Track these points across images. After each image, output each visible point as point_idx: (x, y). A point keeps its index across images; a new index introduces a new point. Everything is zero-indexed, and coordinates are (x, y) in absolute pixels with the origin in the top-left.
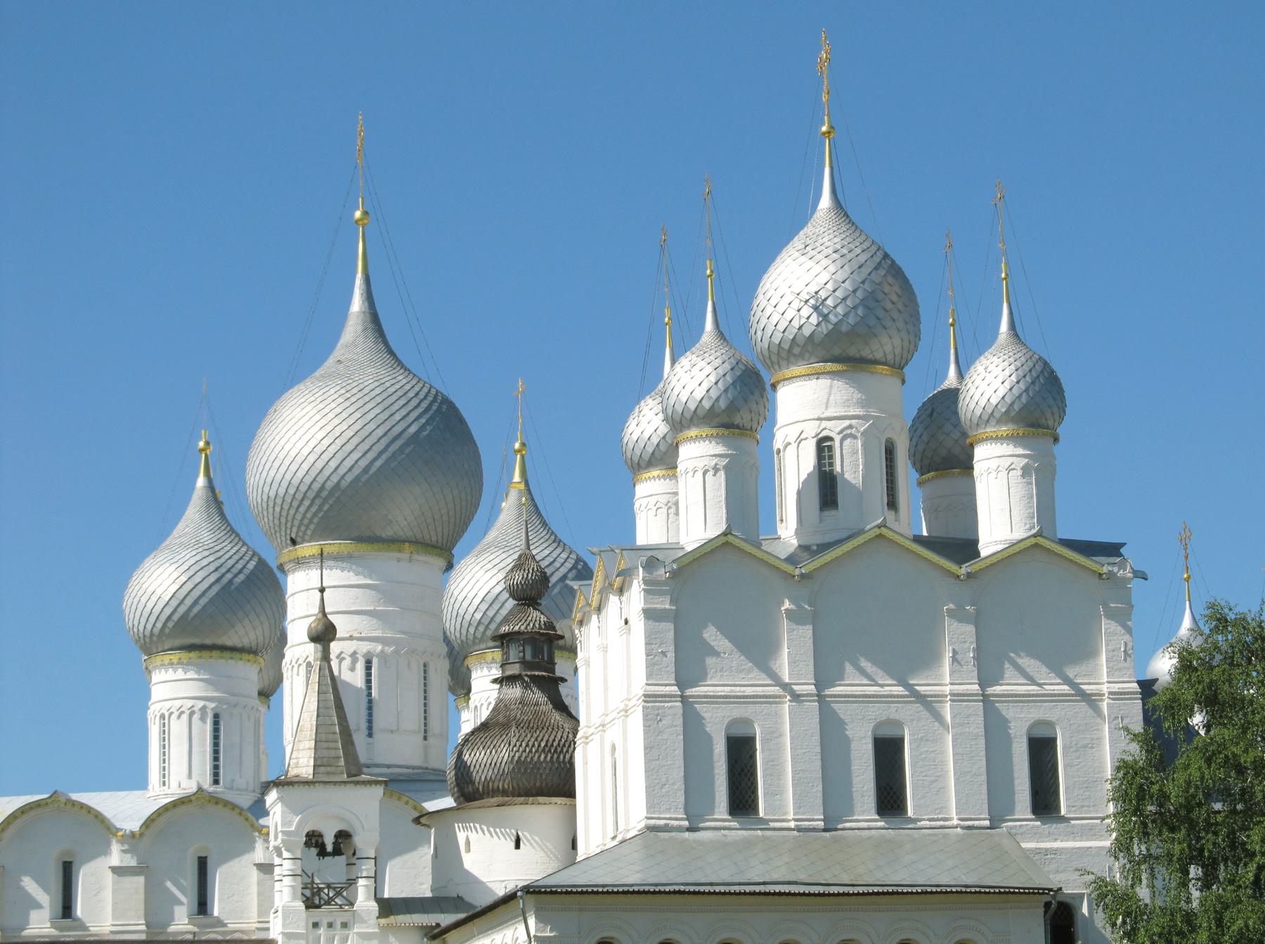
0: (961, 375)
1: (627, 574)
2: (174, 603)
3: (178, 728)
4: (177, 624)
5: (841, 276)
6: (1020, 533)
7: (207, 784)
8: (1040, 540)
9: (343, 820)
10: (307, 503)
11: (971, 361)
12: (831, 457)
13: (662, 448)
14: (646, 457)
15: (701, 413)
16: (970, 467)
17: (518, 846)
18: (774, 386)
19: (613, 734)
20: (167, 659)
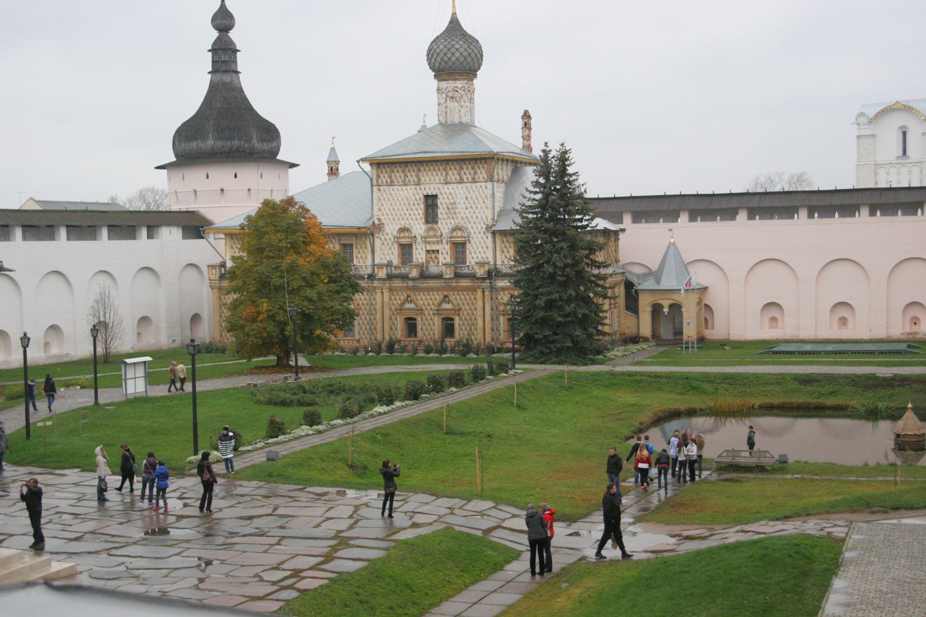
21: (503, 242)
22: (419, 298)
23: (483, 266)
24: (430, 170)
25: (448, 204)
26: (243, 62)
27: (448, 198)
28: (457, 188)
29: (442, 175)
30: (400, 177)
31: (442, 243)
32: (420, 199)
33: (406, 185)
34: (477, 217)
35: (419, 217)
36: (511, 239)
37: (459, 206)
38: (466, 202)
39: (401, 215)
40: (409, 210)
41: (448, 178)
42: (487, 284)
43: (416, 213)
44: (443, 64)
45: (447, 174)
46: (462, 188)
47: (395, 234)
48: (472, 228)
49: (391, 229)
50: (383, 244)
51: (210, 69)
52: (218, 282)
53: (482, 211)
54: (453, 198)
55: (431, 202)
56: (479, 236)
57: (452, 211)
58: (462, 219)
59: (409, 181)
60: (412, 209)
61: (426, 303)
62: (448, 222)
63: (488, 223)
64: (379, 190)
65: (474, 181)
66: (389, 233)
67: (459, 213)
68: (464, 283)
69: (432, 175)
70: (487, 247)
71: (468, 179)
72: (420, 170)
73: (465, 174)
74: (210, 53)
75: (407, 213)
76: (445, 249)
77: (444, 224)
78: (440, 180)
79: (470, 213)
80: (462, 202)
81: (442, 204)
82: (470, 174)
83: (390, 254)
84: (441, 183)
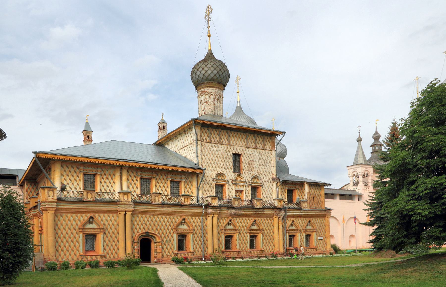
23: (280, 202)
24: (236, 137)
25: (249, 161)
27: (249, 157)
28: (254, 151)
29: (244, 142)
32: (231, 155)
33: (221, 144)
34: (266, 172)
35: (229, 167)
37: (256, 163)
39: (218, 165)
40: (223, 161)
42: (282, 213)
43: (228, 164)
45: (247, 142)
49: (211, 173)
50: (204, 183)
52: (55, 204)
54: (252, 158)
55: (237, 157)
56: (268, 183)
57: (251, 166)
59: (222, 142)
60: (225, 161)
62: (249, 173)
64: (202, 145)
65: (264, 149)
66: (209, 176)
67: (256, 168)
68: (267, 212)
71: (260, 147)
73: (258, 144)
75: (222, 163)
76: (247, 190)
77: (246, 174)
78: (243, 144)
79: (262, 168)
80: (257, 161)
83: (210, 191)
84: (243, 147)
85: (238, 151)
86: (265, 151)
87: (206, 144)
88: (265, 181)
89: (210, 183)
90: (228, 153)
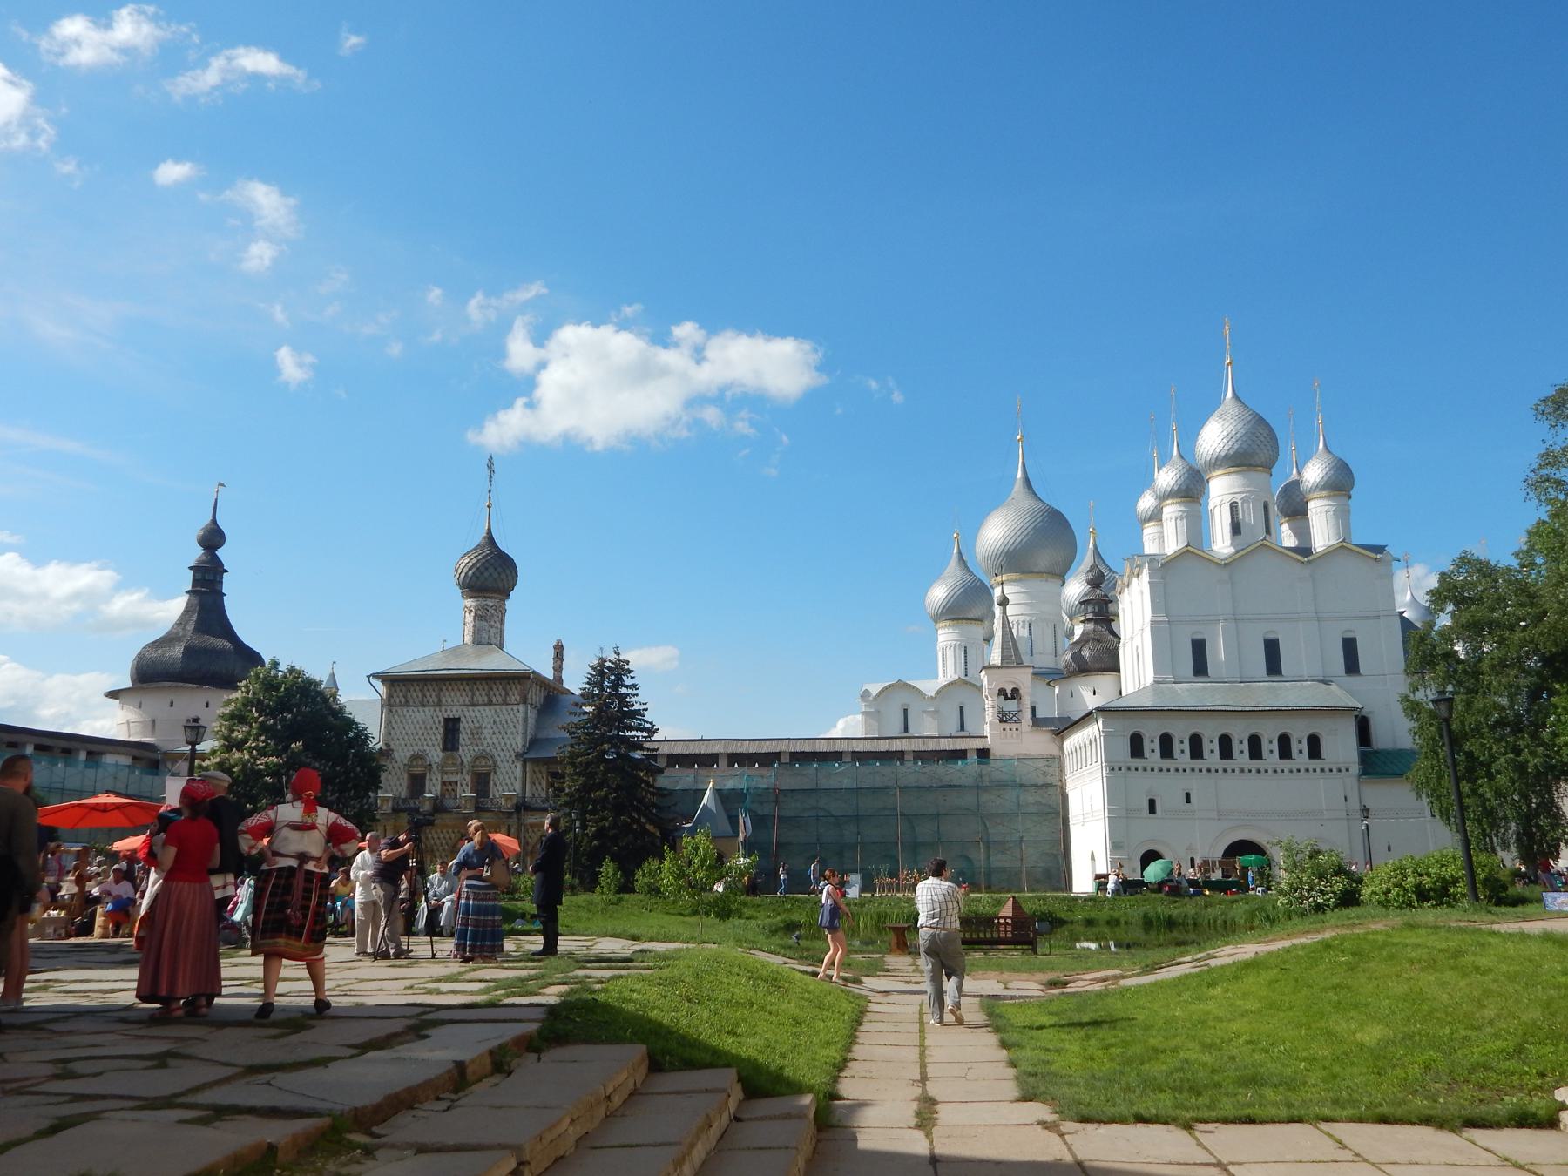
0: (1299, 473)
1: (1141, 567)
2: (947, 600)
3: (950, 653)
4: (947, 610)
5: (1239, 427)
6: (1333, 542)
7: (963, 677)
8: (1345, 544)
9: (1014, 683)
10: (1001, 558)
11: (1305, 463)
12: (1237, 511)
13: (1155, 511)
14: (1148, 517)
15: (1173, 492)
16: (1306, 513)
17: (1094, 694)
18: (1208, 481)
19: (1137, 641)
20: (944, 624)
21: (534, 772)
22: (430, 836)
24: (453, 690)
26: (229, 585)
30: (418, 696)
31: (462, 773)
32: (439, 722)
33: (424, 706)
34: (505, 744)
35: (436, 744)
36: (544, 769)
37: (485, 731)
38: (494, 728)
41: (475, 698)
42: (514, 820)
43: (434, 738)
44: (474, 579)
45: (473, 695)
46: (490, 710)
47: (406, 762)
48: (499, 755)
51: (190, 588)
53: (511, 737)
54: (478, 722)
58: (488, 745)
59: (428, 702)
60: (428, 734)
61: (438, 842)
63: (519, 750)
65: (505, 703)
67: (485, 738)
69: (456, 695)
70: (515, 778)
72: (441, 690)
74: (192, 572)
75: (422, 738)
77: (466, 751)
78: (464, 701)
80: (489, 726)
81: (465, 728)
82: (500, 695)
85: (453, 712)
86: (507, 707)
87: (399, 709)
88: (502, 761)
89: (399, 773)
90: (435, 718)
